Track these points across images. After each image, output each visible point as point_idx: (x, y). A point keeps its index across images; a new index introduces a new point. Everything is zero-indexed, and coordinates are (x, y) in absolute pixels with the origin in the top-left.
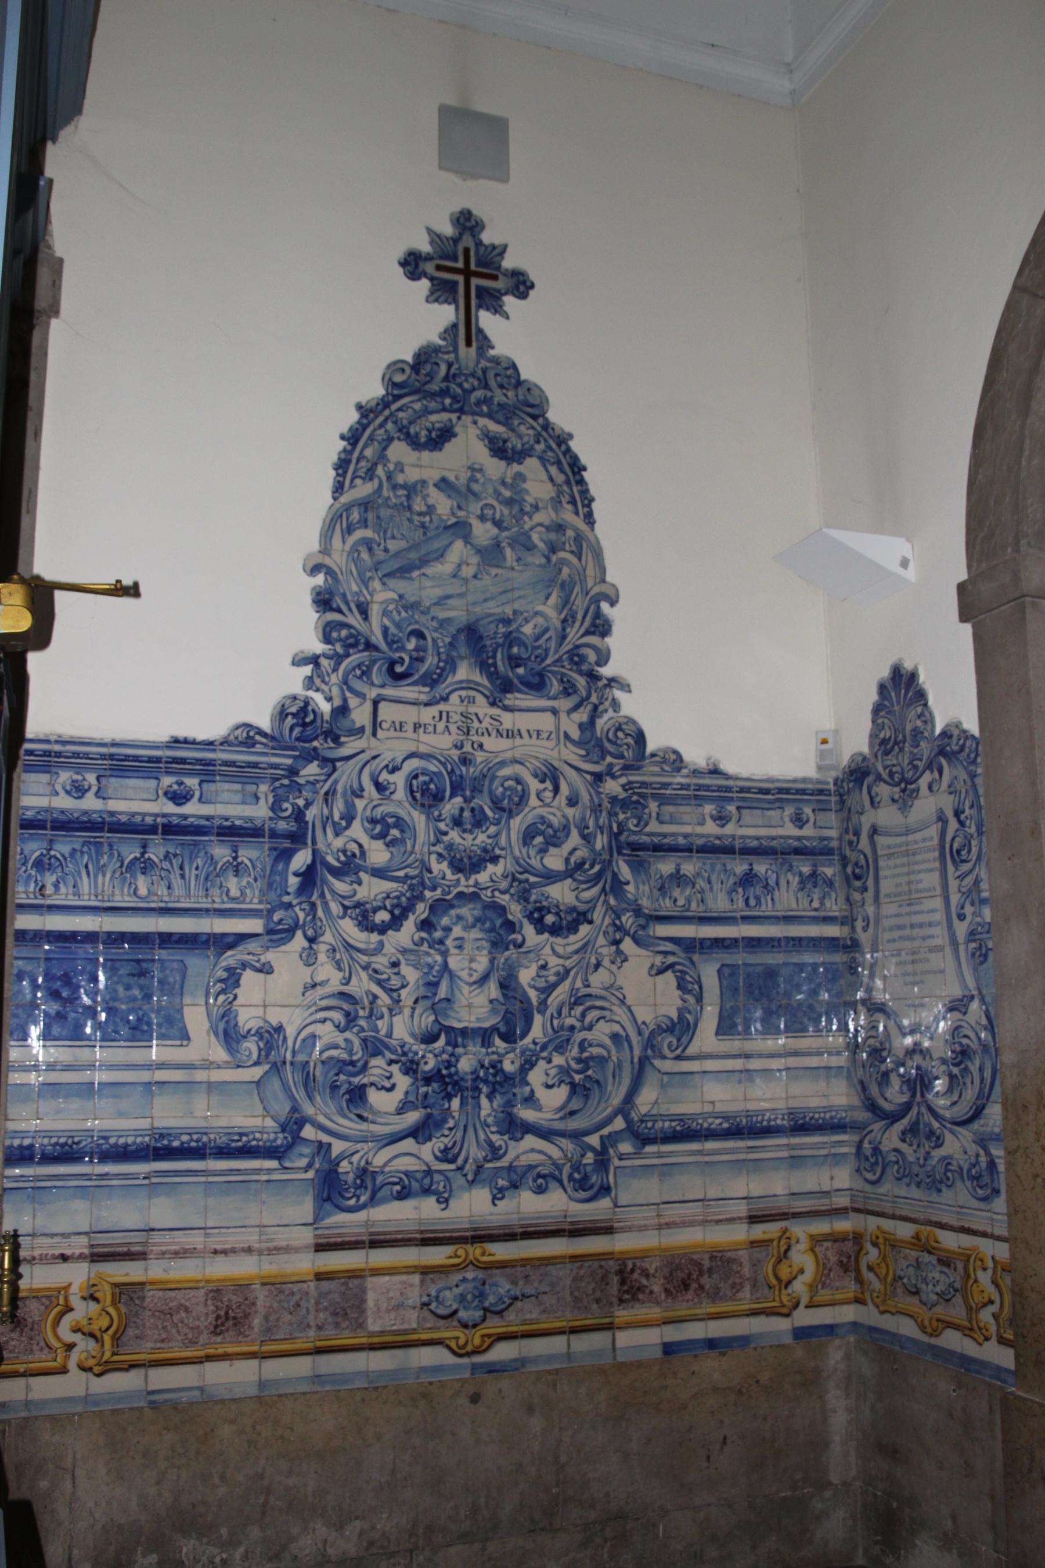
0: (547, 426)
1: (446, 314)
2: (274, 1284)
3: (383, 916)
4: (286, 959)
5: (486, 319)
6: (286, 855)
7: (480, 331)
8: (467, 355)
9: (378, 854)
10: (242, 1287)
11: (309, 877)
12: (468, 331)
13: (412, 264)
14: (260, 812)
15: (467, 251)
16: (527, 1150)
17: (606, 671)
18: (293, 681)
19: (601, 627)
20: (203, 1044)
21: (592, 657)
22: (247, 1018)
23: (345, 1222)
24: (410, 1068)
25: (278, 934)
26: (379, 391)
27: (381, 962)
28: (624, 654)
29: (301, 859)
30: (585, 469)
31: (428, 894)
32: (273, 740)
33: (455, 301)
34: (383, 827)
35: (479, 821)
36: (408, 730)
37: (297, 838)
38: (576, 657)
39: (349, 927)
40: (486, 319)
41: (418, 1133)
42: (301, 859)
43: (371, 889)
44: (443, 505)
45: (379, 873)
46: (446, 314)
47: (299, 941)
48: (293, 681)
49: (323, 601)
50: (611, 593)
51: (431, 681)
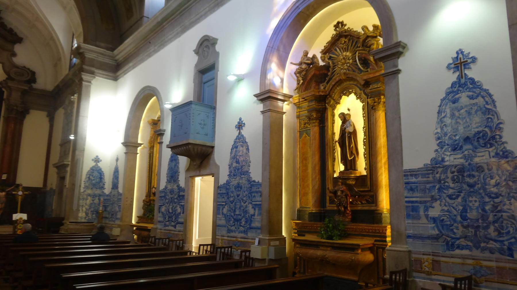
0: (482, 89)
1: (457, 74)
3: (454, 197)
4: (436, 204)
5: (467, 72)
7: (465, 74)
15: (460, 58)
17: (503, 140)
20: (424, 220)
21: (498, 137)
26: (444, 95)
27: (454, 205)
30: (493, 95)
31: (463, 192)
33: (458, 70)
35: (474, 176)
39: (447, 199)
40: (467, 72)
43: (451, 191)
45: (452, 188)
46: (457, 74)
47: (438, 202)
50: (502, 122)
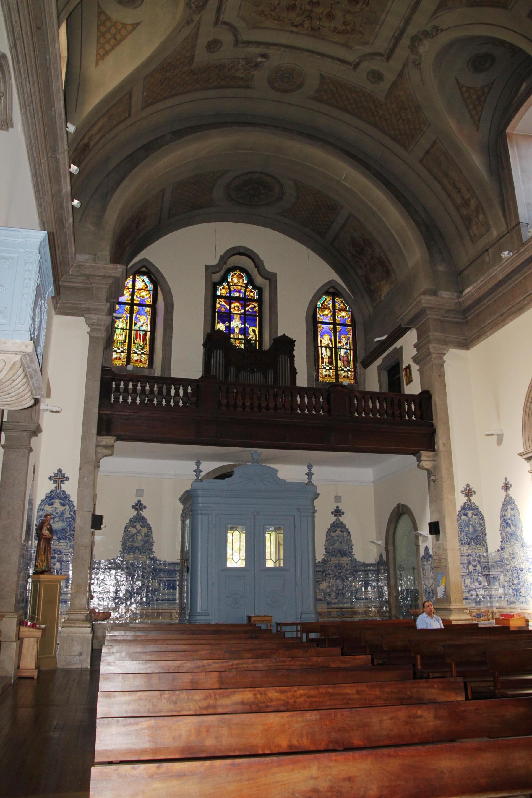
1: (336, 518)
2: (324, 612)
6: (323, 573)
8: (338, 522)
9: (331, 573)
10: (321, 612)
11: (325, 575)
12: (338, 519)
13: (332, 513)
14: (321, 569)
16: (345, 600)
18: (323, 557)
19: (352, 549)
22: (320, 588)
23: (330, 606)
24: (335, 592)
25: (323, 581)
28: (354, 552)
29: (325, 573)
32: (322, 563)
34: (332, 570)
35: (341, 569)
36: (334, 561)
37: (324, 572)
38: (350, 552)
41: (336, 599)
42: (325, 573)
44: (336, 538)
46: (336, 518)
48: (323, 557)
49: (325, 549)
51: (336, 556)
